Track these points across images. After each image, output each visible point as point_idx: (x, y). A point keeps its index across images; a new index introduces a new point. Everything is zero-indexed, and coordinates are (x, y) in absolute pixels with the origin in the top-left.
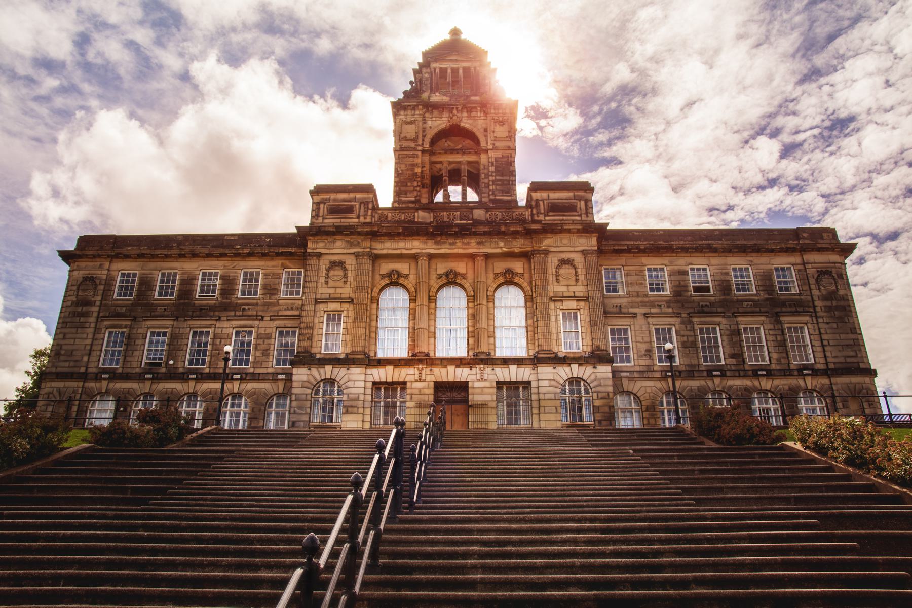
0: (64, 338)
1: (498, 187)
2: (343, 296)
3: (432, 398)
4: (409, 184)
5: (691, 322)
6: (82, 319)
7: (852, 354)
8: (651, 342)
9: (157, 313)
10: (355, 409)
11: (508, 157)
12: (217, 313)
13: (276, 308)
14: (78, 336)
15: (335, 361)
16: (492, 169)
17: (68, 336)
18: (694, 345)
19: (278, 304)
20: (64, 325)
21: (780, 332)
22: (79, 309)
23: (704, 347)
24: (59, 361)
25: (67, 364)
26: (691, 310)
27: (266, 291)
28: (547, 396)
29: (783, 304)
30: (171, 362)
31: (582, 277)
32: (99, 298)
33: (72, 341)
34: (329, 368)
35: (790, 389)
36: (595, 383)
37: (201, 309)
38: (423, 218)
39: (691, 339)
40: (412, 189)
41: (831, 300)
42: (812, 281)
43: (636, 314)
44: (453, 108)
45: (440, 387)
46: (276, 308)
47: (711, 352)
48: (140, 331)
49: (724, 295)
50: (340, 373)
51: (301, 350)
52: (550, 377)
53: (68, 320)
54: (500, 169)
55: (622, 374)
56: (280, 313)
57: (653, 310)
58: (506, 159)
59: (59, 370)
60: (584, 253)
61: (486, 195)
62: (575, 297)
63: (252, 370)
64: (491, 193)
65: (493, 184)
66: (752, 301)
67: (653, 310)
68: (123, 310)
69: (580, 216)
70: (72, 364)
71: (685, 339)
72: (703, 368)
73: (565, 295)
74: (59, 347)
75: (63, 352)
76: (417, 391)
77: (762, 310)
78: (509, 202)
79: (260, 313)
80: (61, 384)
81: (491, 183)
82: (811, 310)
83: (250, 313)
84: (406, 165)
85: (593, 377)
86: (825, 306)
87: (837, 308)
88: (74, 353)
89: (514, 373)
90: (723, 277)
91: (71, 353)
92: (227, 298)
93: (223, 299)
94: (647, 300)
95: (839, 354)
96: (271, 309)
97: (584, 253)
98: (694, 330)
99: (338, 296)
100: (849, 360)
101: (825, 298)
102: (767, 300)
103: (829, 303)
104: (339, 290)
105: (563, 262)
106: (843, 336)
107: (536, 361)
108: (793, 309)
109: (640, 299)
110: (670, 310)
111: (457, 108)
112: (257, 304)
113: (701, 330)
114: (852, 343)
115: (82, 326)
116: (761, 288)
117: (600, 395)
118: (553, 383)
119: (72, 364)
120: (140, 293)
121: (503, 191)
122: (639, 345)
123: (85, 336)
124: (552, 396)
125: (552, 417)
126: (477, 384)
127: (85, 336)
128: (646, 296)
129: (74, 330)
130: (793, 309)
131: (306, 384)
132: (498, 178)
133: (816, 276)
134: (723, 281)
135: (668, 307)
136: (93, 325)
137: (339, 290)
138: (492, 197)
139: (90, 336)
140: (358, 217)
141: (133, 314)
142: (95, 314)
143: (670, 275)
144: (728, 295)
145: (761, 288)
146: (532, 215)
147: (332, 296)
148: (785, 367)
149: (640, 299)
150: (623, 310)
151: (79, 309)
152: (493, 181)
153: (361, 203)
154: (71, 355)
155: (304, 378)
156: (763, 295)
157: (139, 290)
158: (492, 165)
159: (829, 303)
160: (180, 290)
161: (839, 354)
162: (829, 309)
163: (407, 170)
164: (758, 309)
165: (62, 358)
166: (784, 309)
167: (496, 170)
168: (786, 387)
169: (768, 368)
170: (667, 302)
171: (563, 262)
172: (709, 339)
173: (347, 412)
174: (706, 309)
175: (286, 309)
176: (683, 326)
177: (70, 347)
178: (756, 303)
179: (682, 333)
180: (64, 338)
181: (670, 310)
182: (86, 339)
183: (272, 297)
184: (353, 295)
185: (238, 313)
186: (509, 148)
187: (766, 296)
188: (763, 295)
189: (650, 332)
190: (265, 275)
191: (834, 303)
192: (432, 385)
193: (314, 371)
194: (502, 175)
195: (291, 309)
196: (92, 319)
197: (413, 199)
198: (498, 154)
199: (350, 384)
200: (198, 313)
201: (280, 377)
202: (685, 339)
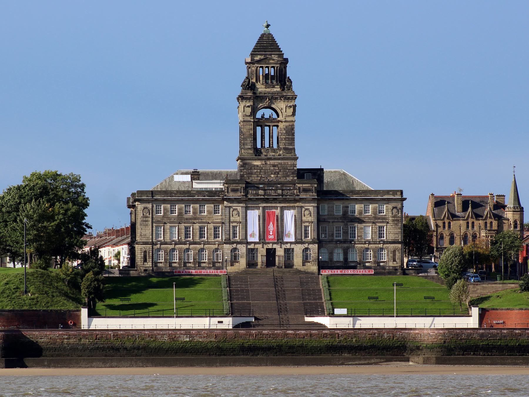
0: (142, 230)
1: (287, 142)
2: (238, 221)
3: (265, 253)
4: (248, 140)
5: (347, 225)
6: (146, 223)
7: (398, 236)
8: (333, 232)
9: (172, 221)
10: (243, 257)
11: (292, 125)
12: (193, 221)
13: (212, 219)
14: (146, 229)
15: (238, 243)
16: (284, 132)
17: (143, 229)
18: (347, 233)
19: (213, 218)
20: (141, 225)
21: (376, 228)
22: (145, 219)
23: (350, 233)
24: (142, 238)
25: (145, 239)
26: (348, 221)
27: (208, 213)
28: (299, 253)
29: (379, 219)
30: (180, 238)
31: (312, 215)
32: (151, 215)
33: (145, 231)
34: (235, 245)
35: (375, 248)
36: (313, 249)
37: (187, 219)
38: (261, 193)
39: (346, 231)
40: (249, 142)
41: (395, 217)
42: (390, 211)
43: (330, 222)
44: (267, 98)
45: (268, 250)
46: (212, 219)
47: (353, 234)
48: (167, 227)
49: (360, 215)
50: (239, 246)
51: (226, 238)
52: (300, 247)
53: (142, 223)
54: (288, 132)
55: (323, 242)
56: (214, 221)
57: (336, 220)
58: (290, 127)
59: (143, 241)
60: (314, 207)
61: (282, 144)
62: (309, 221)
63: (207, 241)
64: (283, 144)
65: (285, 140)
66: (369, 217)
67: (336, 220)
68: (160, 219)
69: (313, 193)
70: (147, 239)
71: (345, 230)
72: (349, 240)
73: (306, 221)
74: (140, 233)
75: (142, 235)
76: (261, 251)
77: (372, 221)
78: (291, 149)
79: (208, 221)
80: (144, 246)
81: (284, 139)
82: (388, 221)
83: (204, 221)
84: (246, 129)
85: (312, 247)
86: (392, 220)
87: (396, 220)
88: (147, 235)
89: (288, 246)
90: (360, 209)
91: (145, 235)
92: (195, 215)
93: (194, 216)
94: (334, 217)
95: (393, 236)
96: (210, 219)
97: (314, 207)
98: (348, 227)
99: (236, 220)
100: (396, 238)
101: (393, 217)
102: (374, 217)
103: (394, 219)
104: (236, 219)
105: (306, 209)
106: (396, 230)
107: (296, 243)
108: (382, 221)
109: (331, 217)
110: (341, 220)
111: (269, 98)
112: (206, 217)
113: (350, 227)
114: (398, 232)
115: (147, 225)
116: (372, 213)
117: (314, 253)
118: (300, 249)
119: (147, 239)
120: (164, 213)
121: (289, 143)
122: (330, 233)
123: (149, 229)
124: (300, 253)
125: (300, 259)
126: (278, 249)
127: (149, 229)
128: (334, 215)
129: (144, 227)
130: (382, 221)
131: (229, 249)
132: (287, 137)
133: (391, 209)
134: (360, 210)
135: (341, 219)
136: (151, 225)
137: (236, 219)
138: (284, 146)
139: (151, 229)
140: (241, 193)
141: (164, 221)
142: (151, 221)
143: (342, 208)
144: (361, 215)
145: (372, 213)
146: (297, 192)
147: (234, 221)
148: (375, 240)
149: (331, 217)
150: (326, 220)
151: (145, 219)
152: (285, 138)
153: (241, 187)
154: (145, 235)
155: (228, 247)
156: (373, 215)
157: (164, 212)
158: (285, 130)
159: (394, 219)
160: (178, 212)
161: (393, 236)
162: (393, 221)
163: (247, 132)
164: (370, 221)
165: (143, 237)
166: (379, 221)
167: (286, 133)
168: (374, 247)
169: (370, 241)
170: (340, 217)
171: (306, 209)
172: (353, 230)
173: (241, 258)
174: (353, 220)
175: (216, 219)
176: (345, 226)
177: (144, 233)
178: (369, 218)
179: (344, 228)
180: (142, 230)
181: (341, 220)
182: (149, 230)
183: (211, 215)
184: (241, 221)
185: (200, 221)
186: (292, 121)
187: (374, 216)
188: (373, 215)
189: (334, 228)
190: (207, 207)
191: (396, 219)
192: (265, 249)
193: (231, 246)
194: (289, 135)
195: (218, 219)
196: (150, 223)
197: (250, 147)
198: (287, 124)
199: (242, 249)
200: (186, 221)
201: (216, 243)
202: (345, 230)
